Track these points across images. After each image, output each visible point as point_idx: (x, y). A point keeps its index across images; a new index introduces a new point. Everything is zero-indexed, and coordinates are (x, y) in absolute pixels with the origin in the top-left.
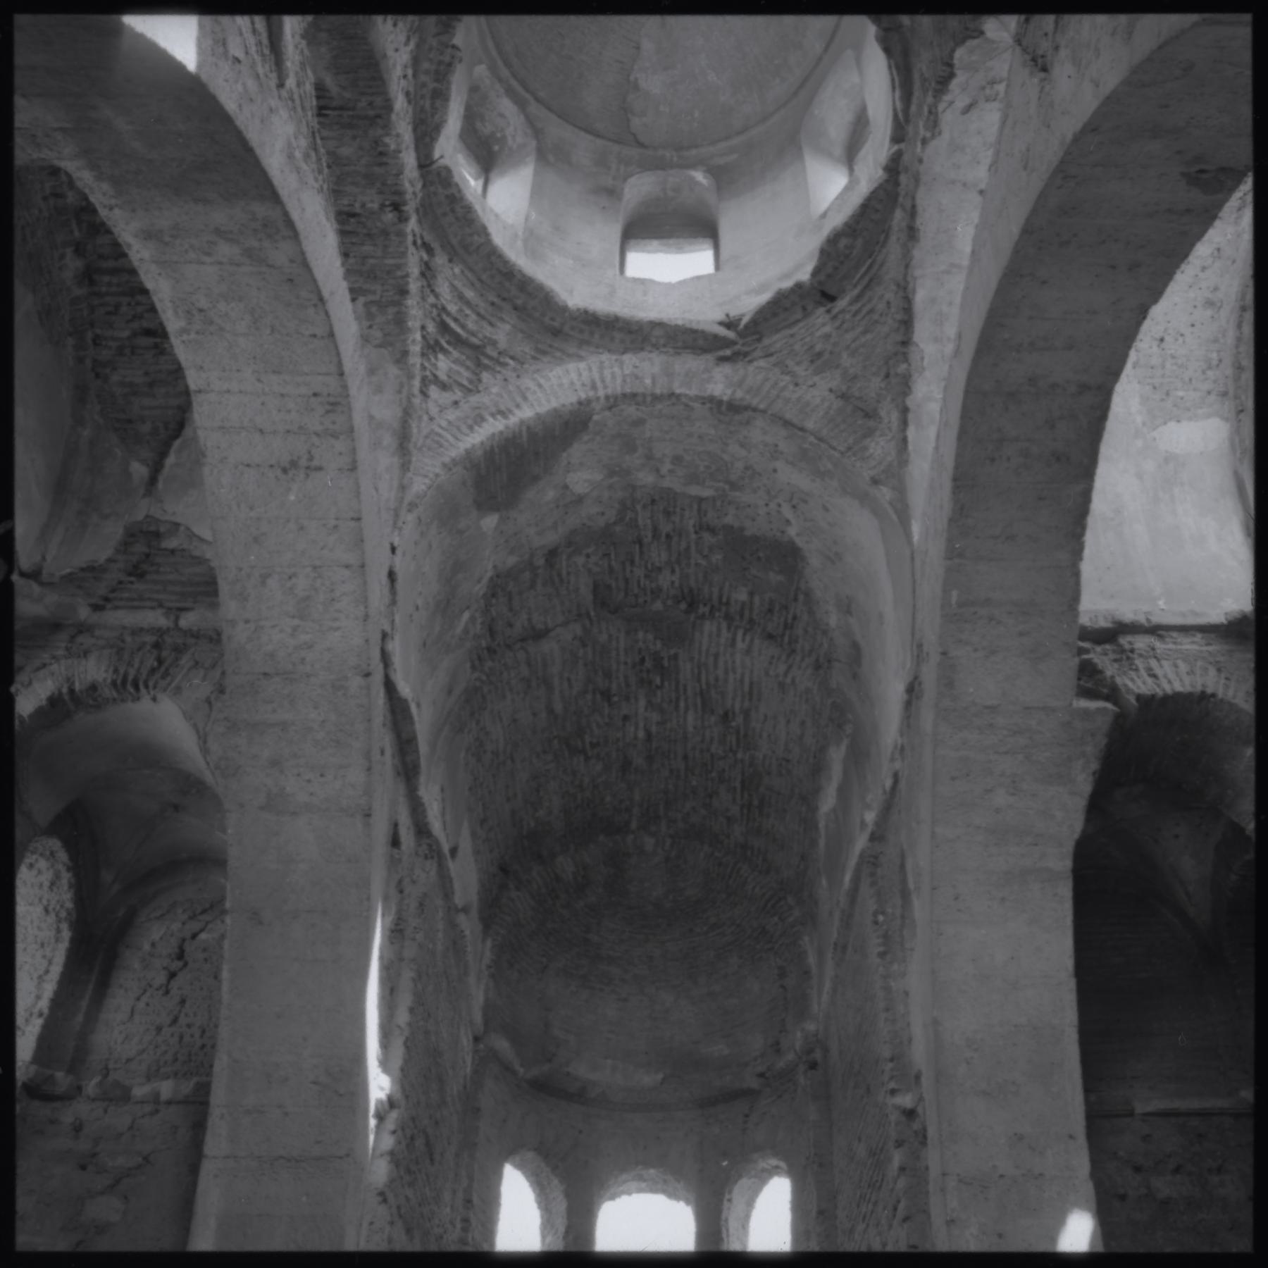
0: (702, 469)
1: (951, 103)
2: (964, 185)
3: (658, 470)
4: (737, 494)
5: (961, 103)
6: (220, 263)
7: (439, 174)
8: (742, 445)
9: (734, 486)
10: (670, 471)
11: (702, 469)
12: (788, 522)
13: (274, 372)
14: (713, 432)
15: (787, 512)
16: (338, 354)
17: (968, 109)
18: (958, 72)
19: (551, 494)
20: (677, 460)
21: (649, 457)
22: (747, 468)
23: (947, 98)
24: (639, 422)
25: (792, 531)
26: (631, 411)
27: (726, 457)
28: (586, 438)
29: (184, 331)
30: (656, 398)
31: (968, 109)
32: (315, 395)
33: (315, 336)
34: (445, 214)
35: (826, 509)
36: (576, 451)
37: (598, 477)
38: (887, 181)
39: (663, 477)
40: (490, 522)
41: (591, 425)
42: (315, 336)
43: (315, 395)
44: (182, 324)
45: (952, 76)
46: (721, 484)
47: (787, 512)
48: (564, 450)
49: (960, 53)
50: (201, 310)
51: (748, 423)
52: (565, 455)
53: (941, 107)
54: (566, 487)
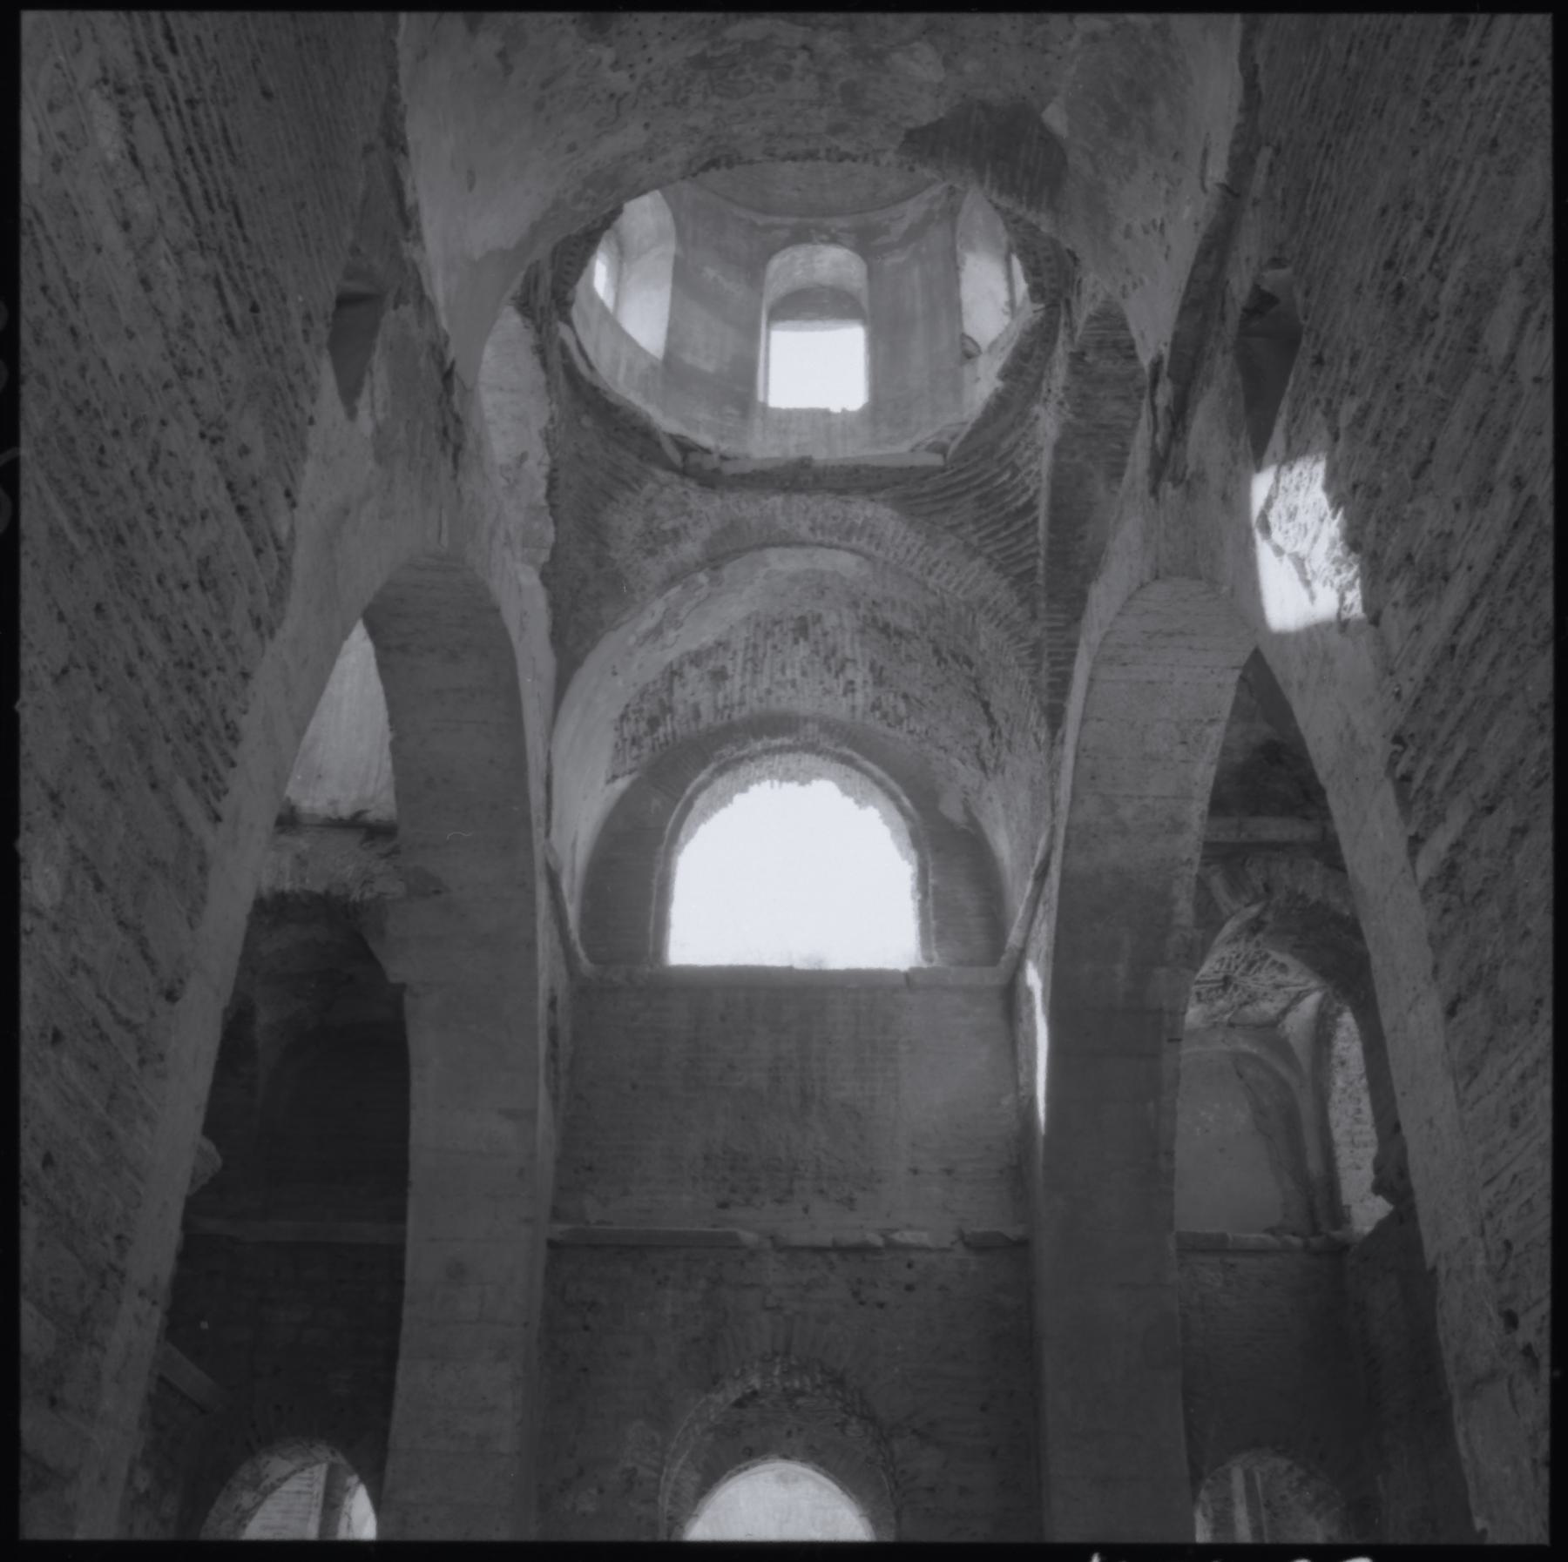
0: (748, 67)
1: (540, 464)
2: (501, 389)
3: (812, 57)
4: (694, 52)
5: (530, 463)
6: (1140, 798)
7: (1043, 297)
8: (695, 129)
9: (702, 62)
10: (793, 56)
11: (748, 67)
12: (615, 66)
13: (1150, 682)
14: (736, 129)
15: (619, 81)
16: (1086, 700)
17: (523, 457)
18: (544, 503)
19: (970, 66)
20: (783, 74)
21: (824, 77)
22: (685, 100)
23: (545, 470)
24: (836, 129)
25: (608, 55)
26: (847, 146)
27: (715, 100)
28: (910, 125)
29: (1212, 721)
30: (812, 155)
31: (523, 457)
32: (1125, 664)
33: (1099, 720)
34: (1048, 259)
35: (572, 148)
36: (925, 112)
37: (897, 58)
38: (565, 293)
39: (804, 47)
40: (1055, 118)
41: (901, 139)
42: (1099, 720)
43: (1125, 664)
44: (1209, 730)
45: (548, 496)
46: (718, 53)
47: (619, 81)
48: (941, 120)
49: (550, 535)
50: (1184, 743)
51: (690, 163)
52: (941, 114)
53: (547, 459)
54: (947, 63)
